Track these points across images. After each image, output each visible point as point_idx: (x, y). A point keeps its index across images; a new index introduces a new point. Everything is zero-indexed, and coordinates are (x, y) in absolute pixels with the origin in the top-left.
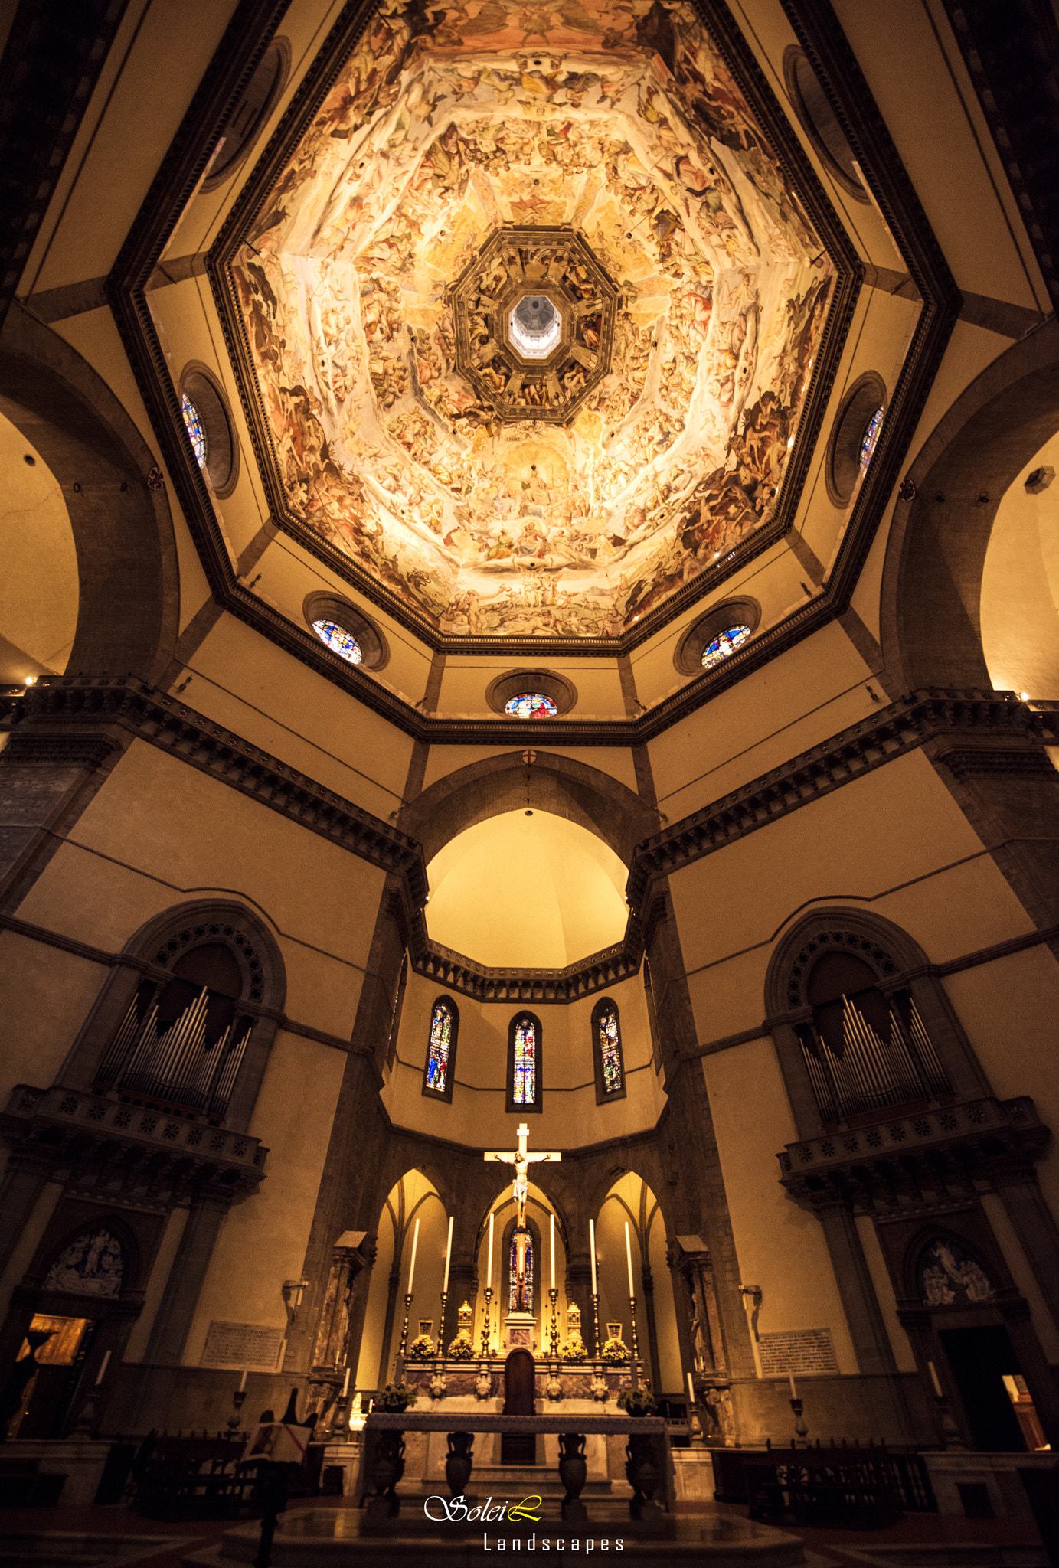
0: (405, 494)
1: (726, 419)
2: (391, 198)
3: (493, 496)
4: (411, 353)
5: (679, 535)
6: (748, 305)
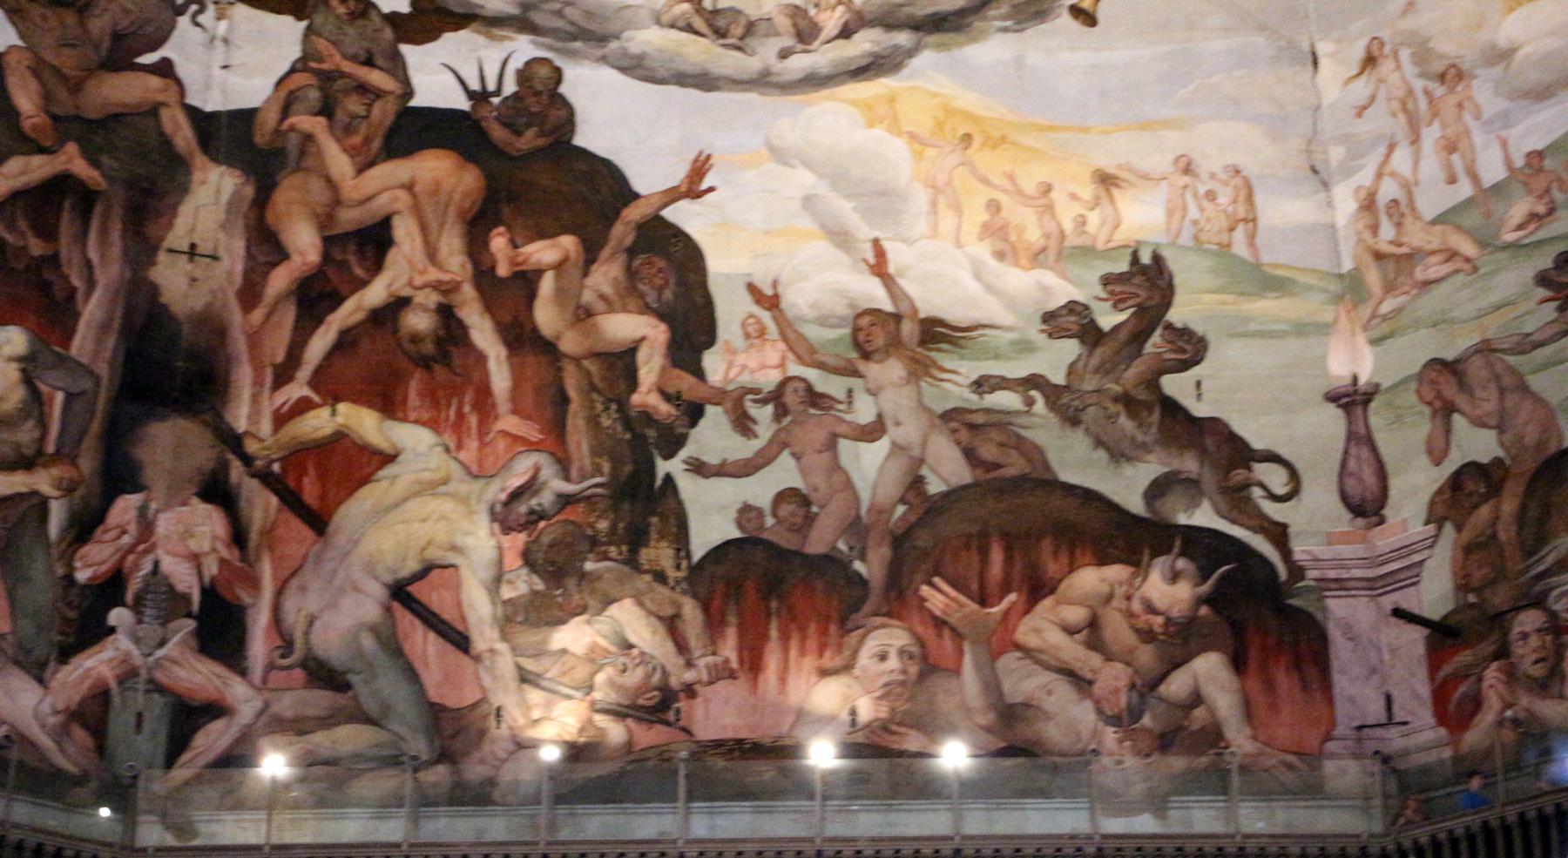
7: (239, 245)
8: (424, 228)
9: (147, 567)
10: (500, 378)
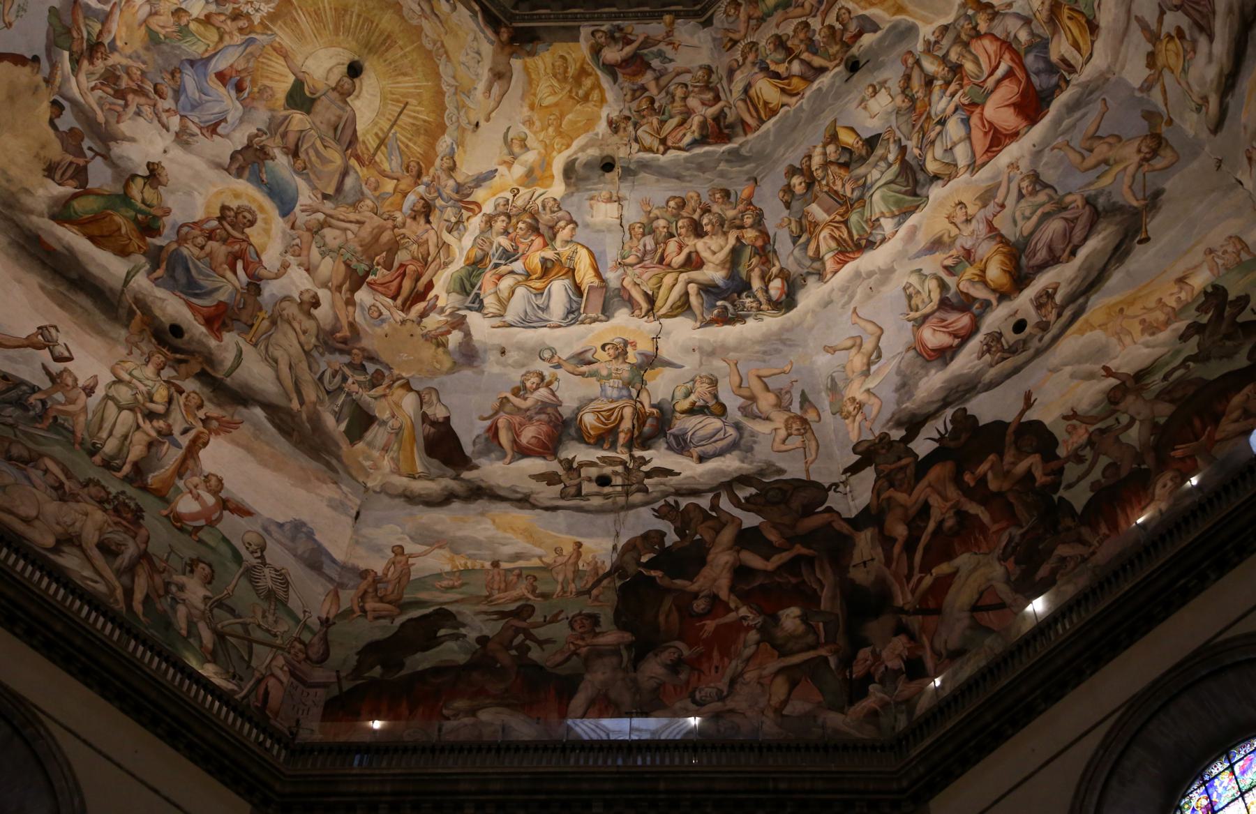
1: (905, 386)
3: (196, 49)
5: (618, 569)
6: (1116, 198)
7: (880, 549)
8: (939, 494)
9: (882, 669)
10: (985, 517)
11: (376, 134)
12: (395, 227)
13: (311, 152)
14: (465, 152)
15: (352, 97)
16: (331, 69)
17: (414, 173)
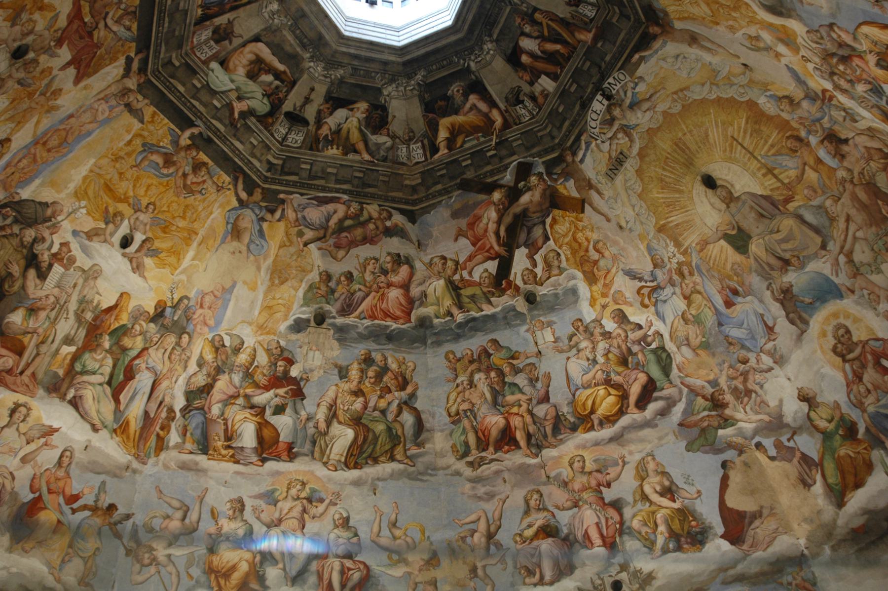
0: (587, 541)
2: (31, 421)
3: (710, 319)
4: (342, 333)
11: (764, 175)
12: (852, 181)
13: (785, 246)
14: (773, 83)
15: (733, 191)
16: (711, 205)
17: (797, 144)
